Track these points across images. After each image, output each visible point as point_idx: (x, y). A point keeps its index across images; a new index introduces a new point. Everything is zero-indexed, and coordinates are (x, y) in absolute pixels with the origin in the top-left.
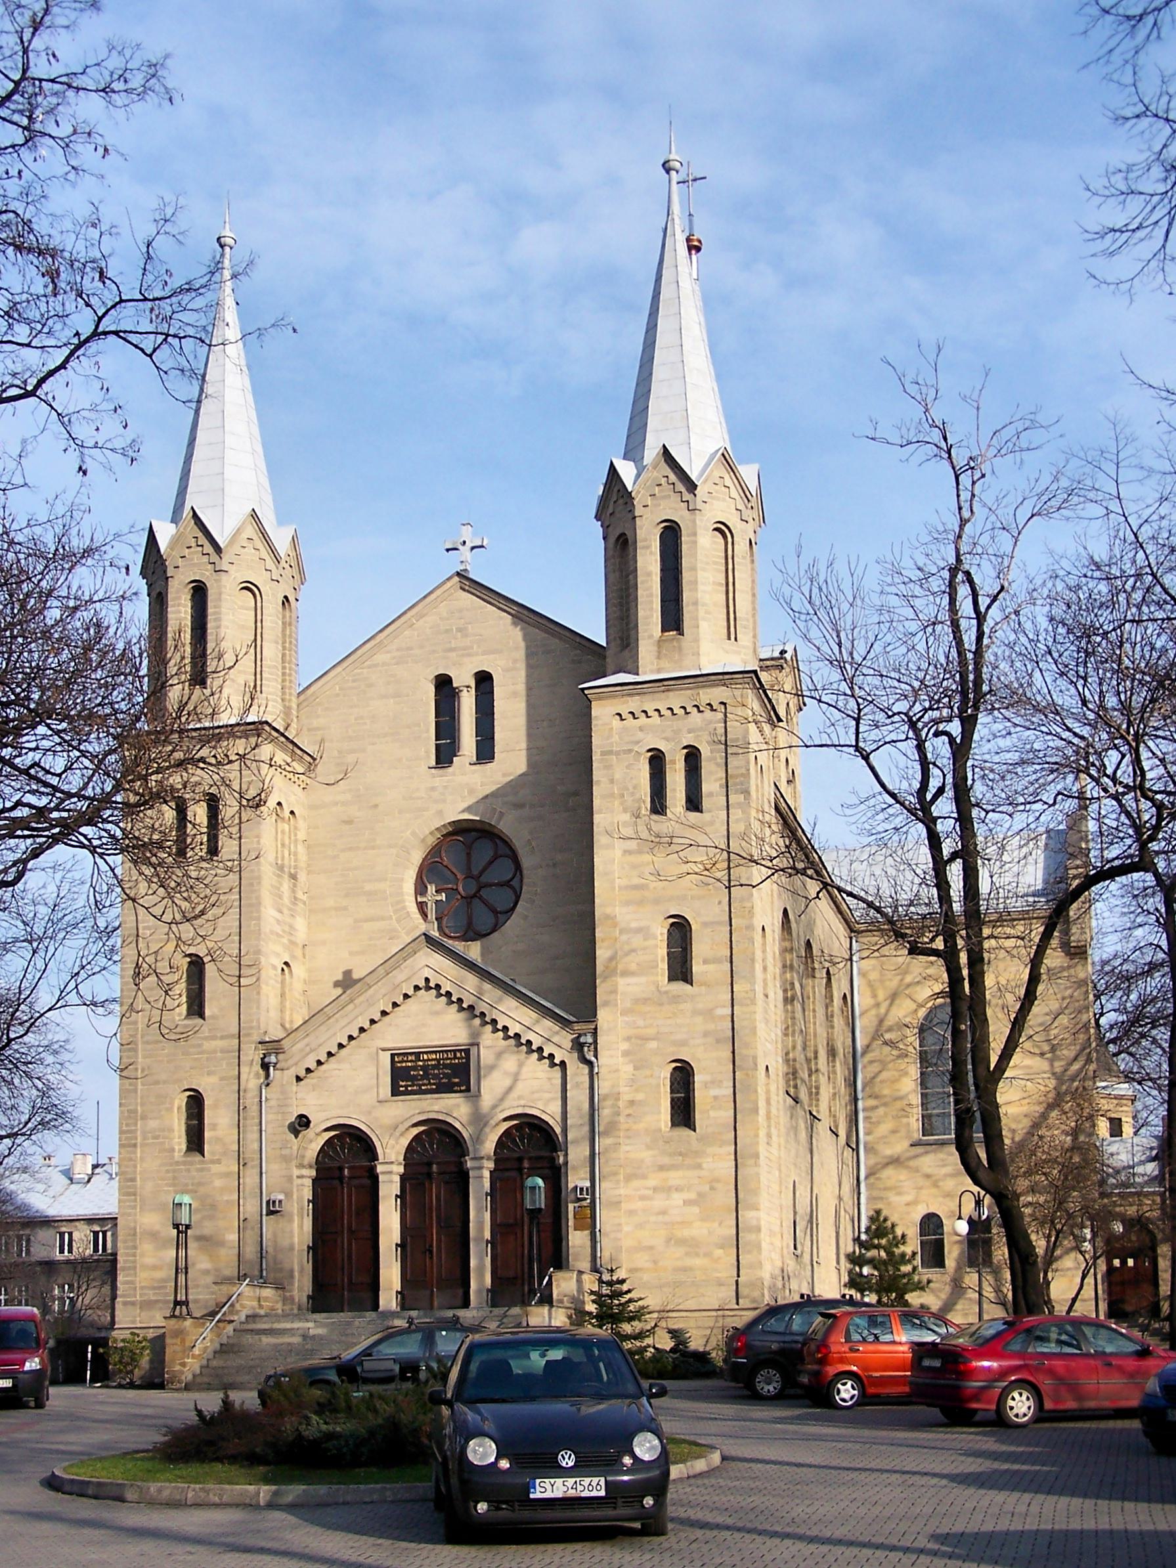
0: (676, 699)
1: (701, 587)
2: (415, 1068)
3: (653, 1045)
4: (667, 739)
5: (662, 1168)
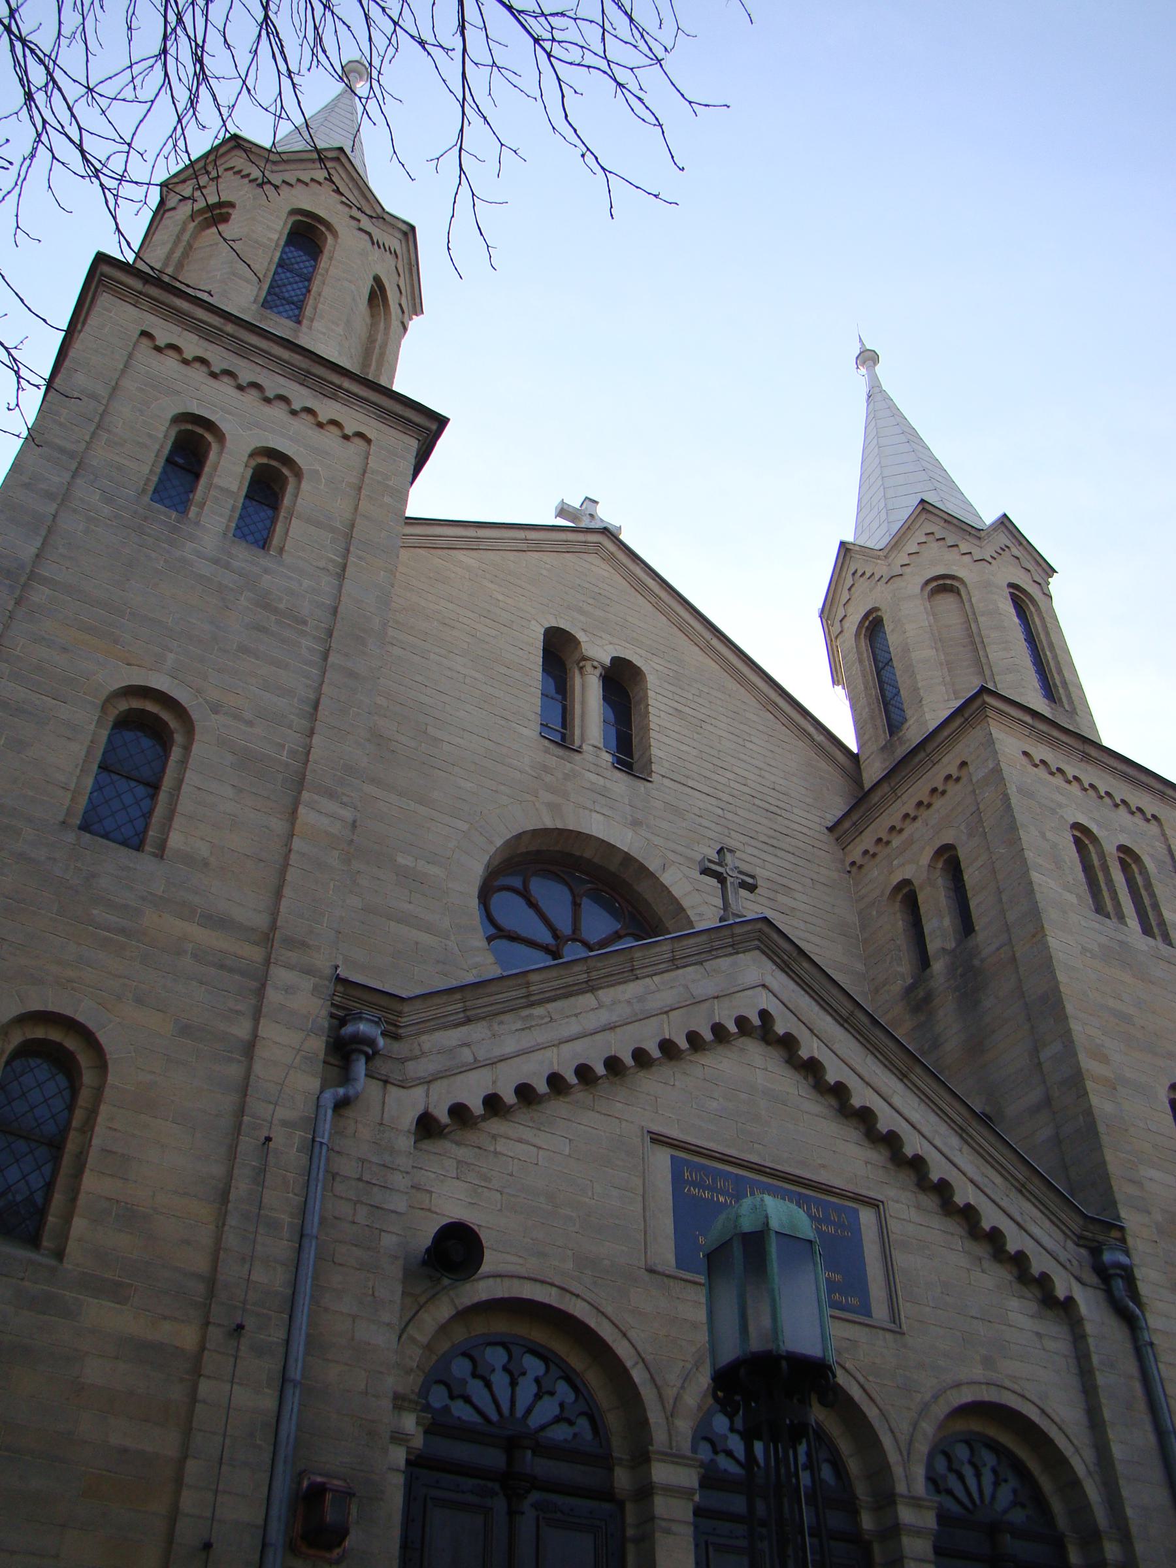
4: (1099, 825)
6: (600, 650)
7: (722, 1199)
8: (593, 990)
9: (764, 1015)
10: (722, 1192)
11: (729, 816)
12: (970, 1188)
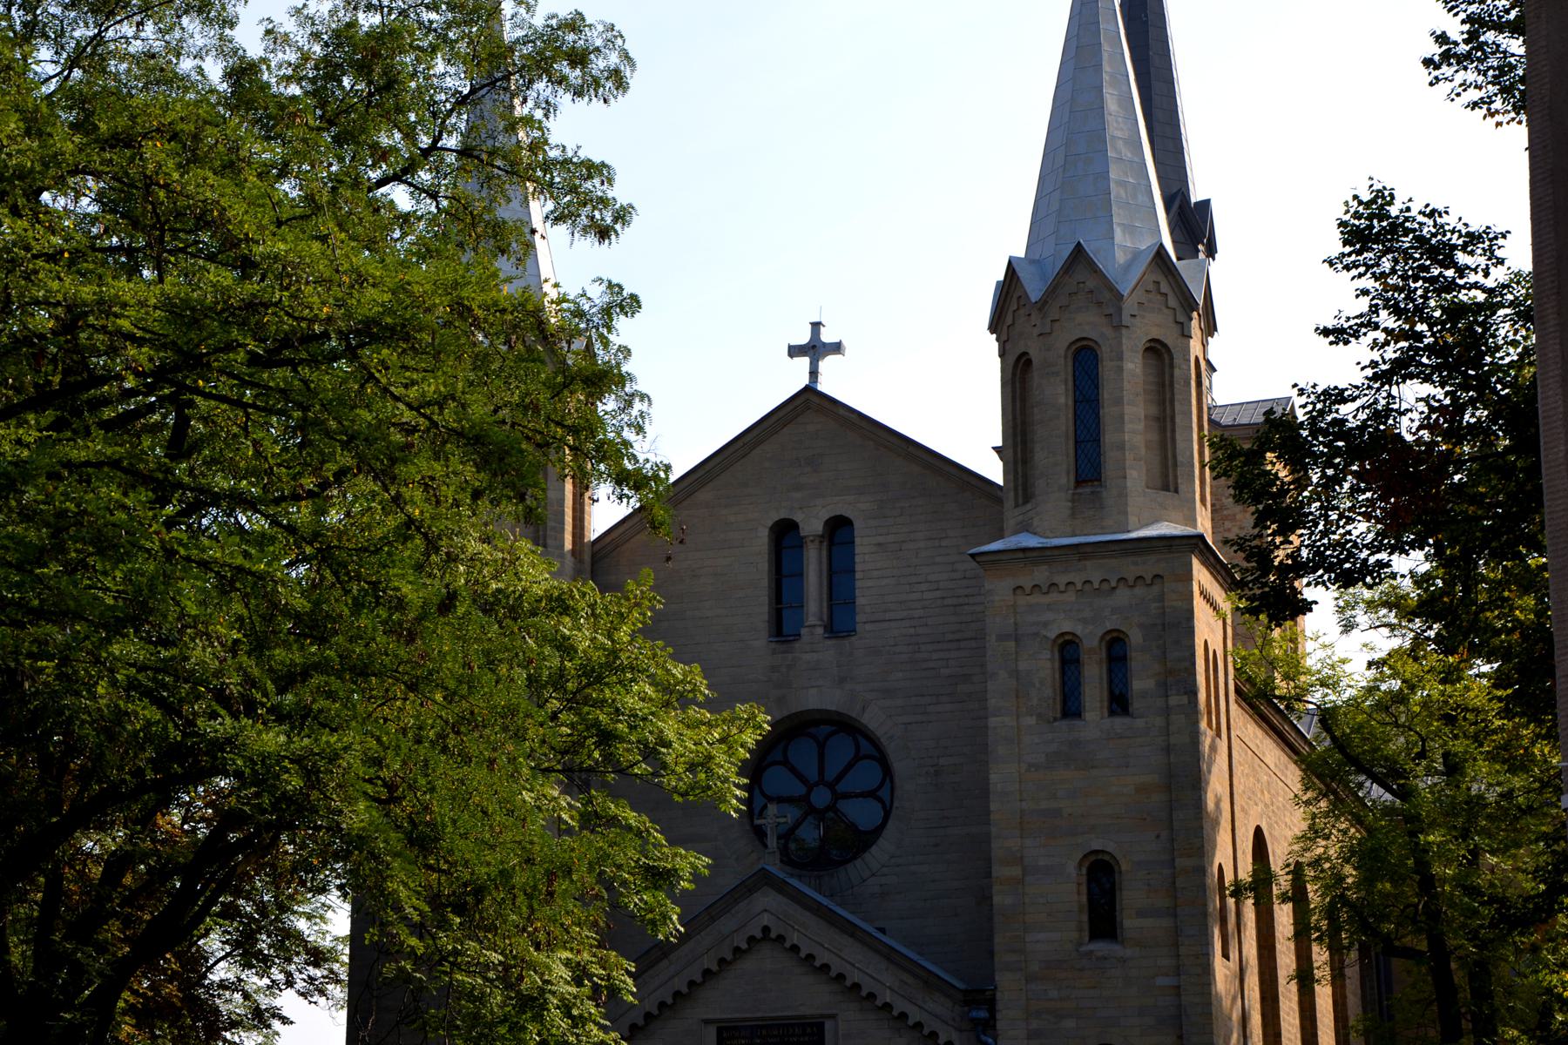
0: (1094, 571)
1: (1128, 427)
3: (1070, 1024)
6: (812, 524)
9: (766, 929)
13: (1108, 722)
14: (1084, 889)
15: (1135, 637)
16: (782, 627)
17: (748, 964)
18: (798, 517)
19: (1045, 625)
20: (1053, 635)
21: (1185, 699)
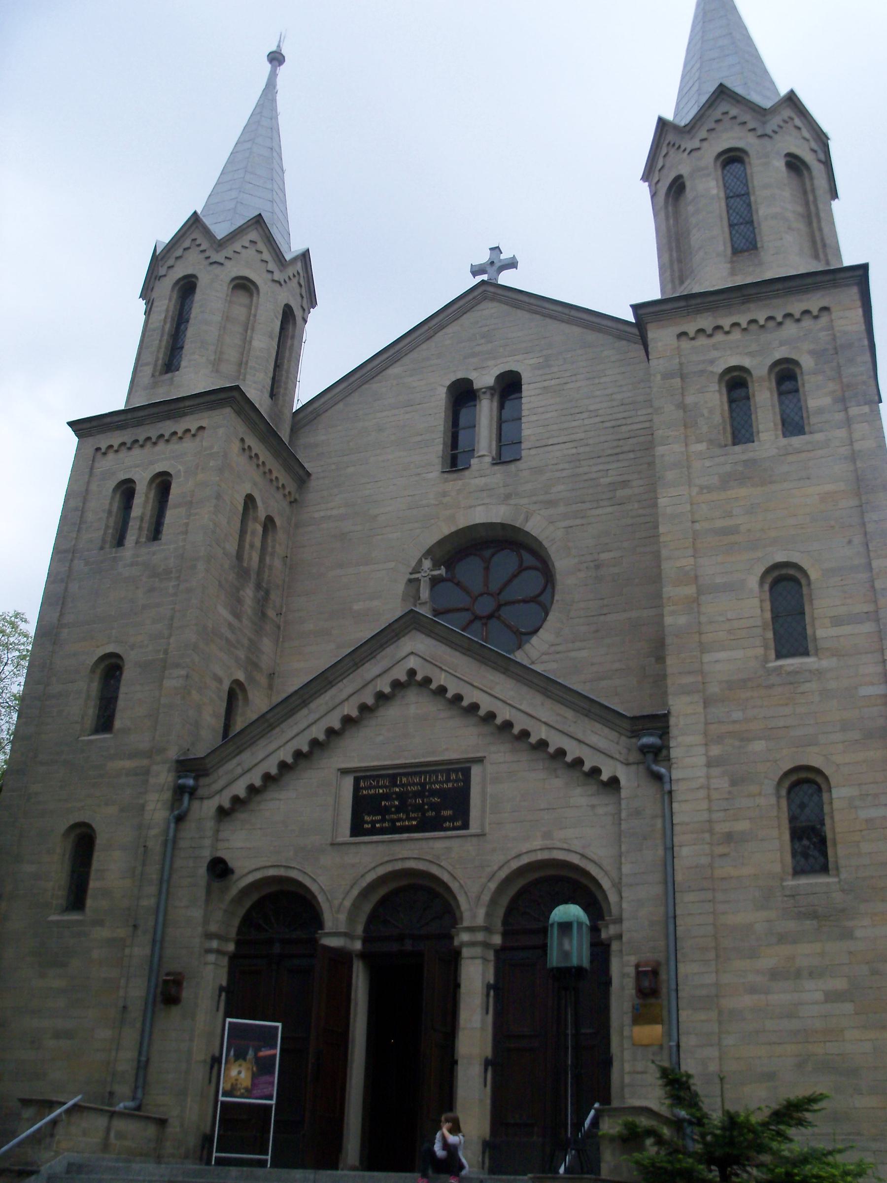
2: (385, 797)
3: (759, 746)
4: (751, 354)
5: (782, 939)
6: (484, 379)
7: (381, 791)
8: (306, 705)
10: (381, 787)
11: (581, 450)
12: (544, 728)
13: (784, 441)
14: (767, 605)
15: (807, 362)
16: (456, 460)
17: (391, 712)
18: (472, 376)
19: (712, 362)
20: (720, 368)
21: (866, 409)
